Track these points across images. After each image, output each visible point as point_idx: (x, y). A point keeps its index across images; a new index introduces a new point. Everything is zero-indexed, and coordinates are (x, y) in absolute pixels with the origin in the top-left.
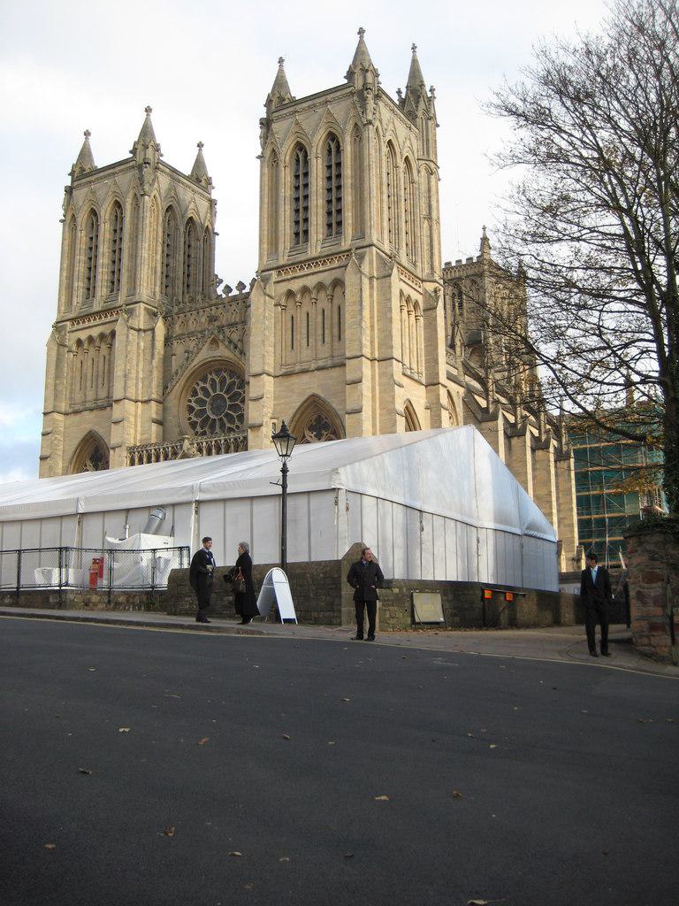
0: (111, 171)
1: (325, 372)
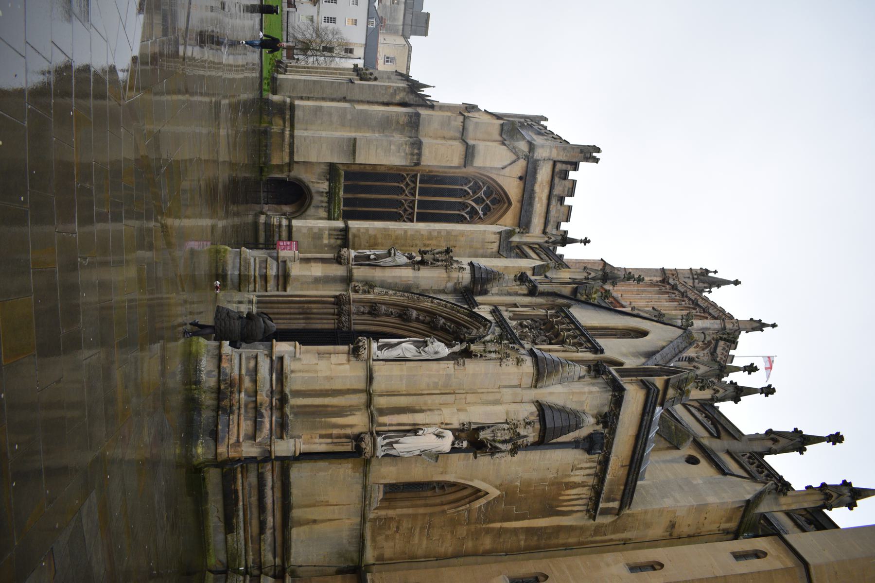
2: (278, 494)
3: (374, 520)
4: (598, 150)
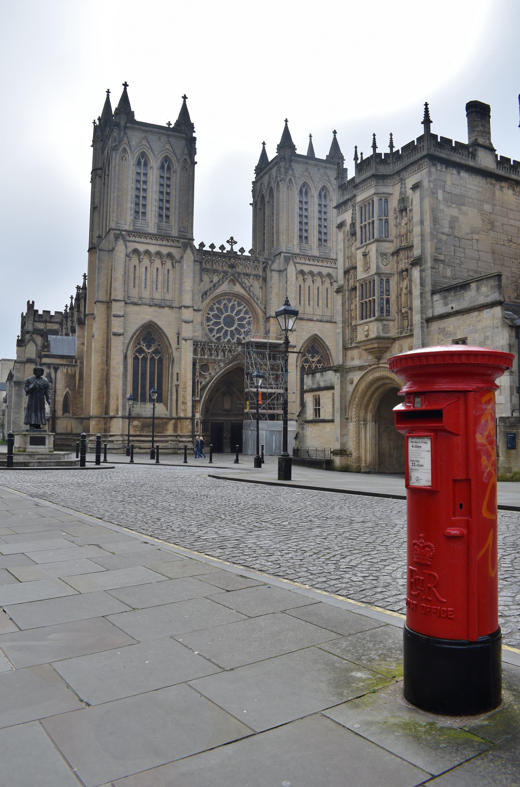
0: (164, 131)
1: (322, 323)
4: (28, 302)
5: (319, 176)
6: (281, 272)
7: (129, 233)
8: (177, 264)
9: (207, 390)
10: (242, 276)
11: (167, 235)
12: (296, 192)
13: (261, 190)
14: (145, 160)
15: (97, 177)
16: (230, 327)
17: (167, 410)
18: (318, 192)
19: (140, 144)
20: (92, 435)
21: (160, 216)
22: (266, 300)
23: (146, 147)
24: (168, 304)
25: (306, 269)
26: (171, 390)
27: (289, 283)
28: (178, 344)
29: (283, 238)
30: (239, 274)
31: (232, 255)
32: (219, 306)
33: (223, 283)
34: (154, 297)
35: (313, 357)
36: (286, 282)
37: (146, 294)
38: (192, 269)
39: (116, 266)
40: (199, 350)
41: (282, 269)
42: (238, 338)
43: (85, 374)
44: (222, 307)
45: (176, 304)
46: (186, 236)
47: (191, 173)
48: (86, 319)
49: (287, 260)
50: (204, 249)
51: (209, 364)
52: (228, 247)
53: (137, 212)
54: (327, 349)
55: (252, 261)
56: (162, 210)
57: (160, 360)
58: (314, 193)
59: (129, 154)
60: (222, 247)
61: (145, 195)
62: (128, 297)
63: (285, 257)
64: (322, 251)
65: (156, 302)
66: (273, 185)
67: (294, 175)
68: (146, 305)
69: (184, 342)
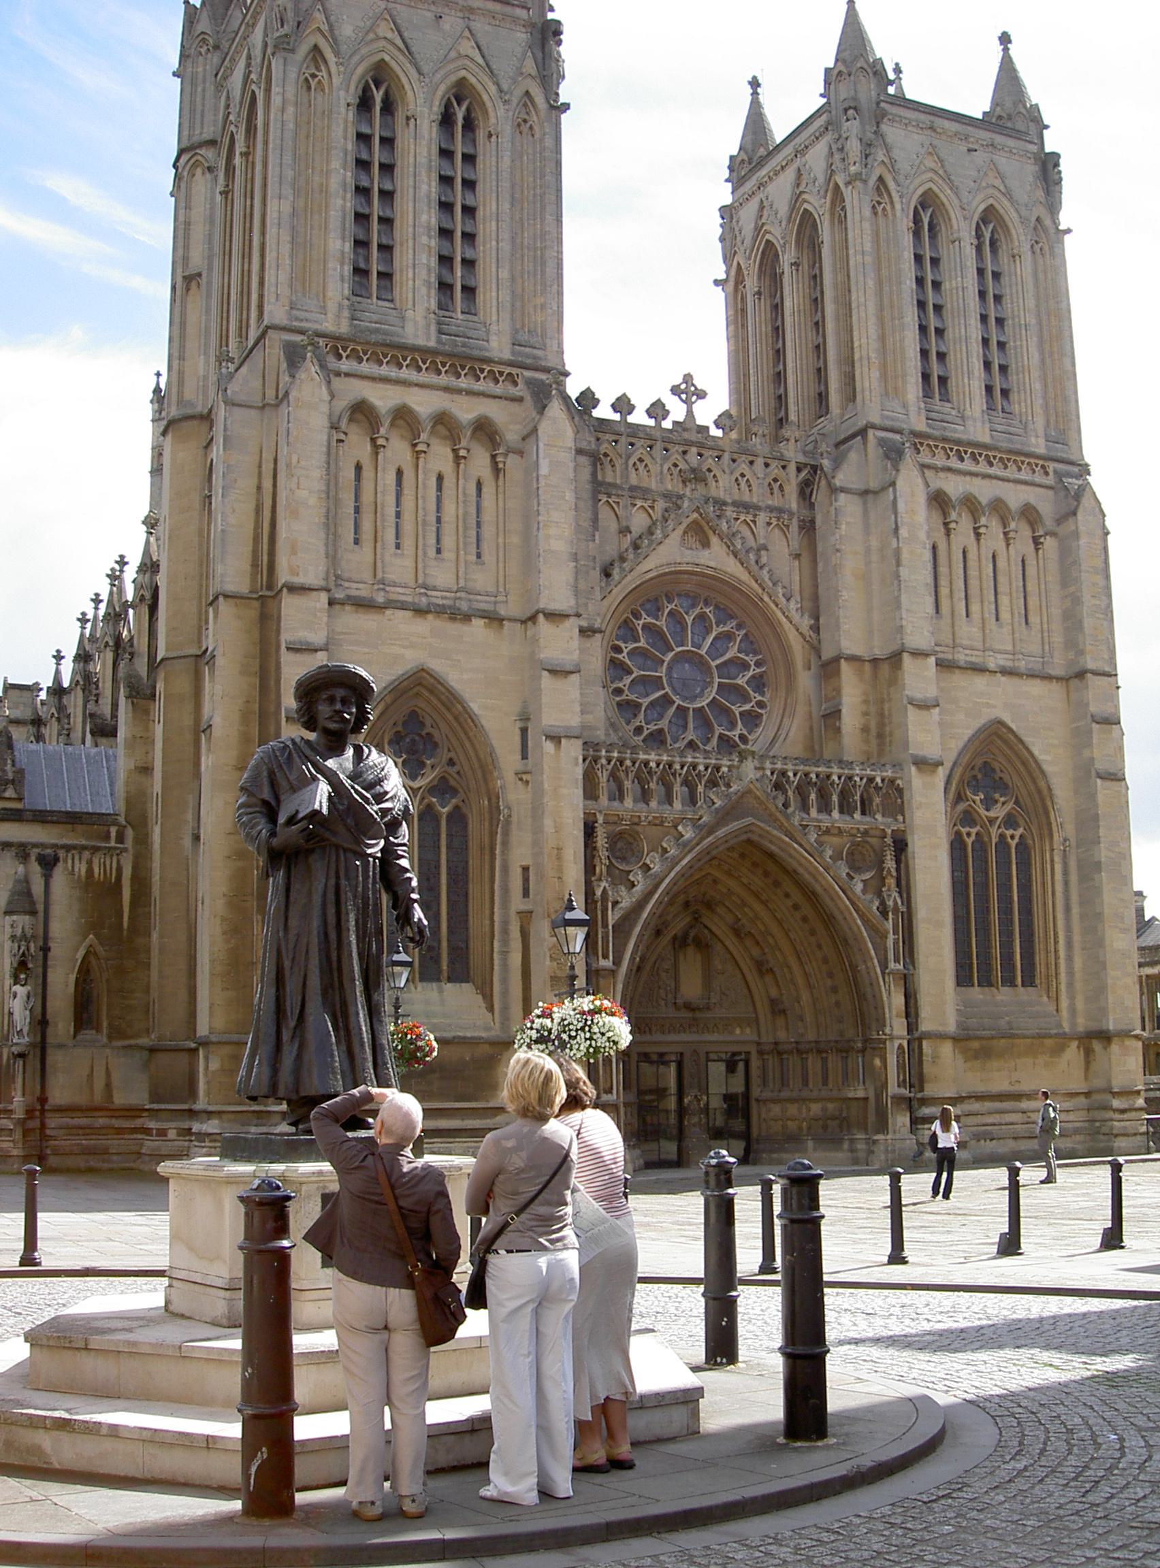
1: (1015, 681)
2: (79, 1114)
3: (110, 1038)
5: (974, 174)
6: (870, 497)
7: (338, 345)
8: (512, 461)
9: (637, 929)
10: (730, 512)
11: (476, 353)
12: (905, 223)
13: (758, 229)
14: (387, 94)
15: (199, 171)
16: (693, 699)
17: (491, 1009)
18: (974, 227)
19: (371, 36)
20: (210, 1114)
21: (445, 287)
22: (815, 598)
23: (390, 47)
24: (483, 606)
25: (954, 487)
26: (505, 932)
27: (903, 532)
28: (524, 757)
29: (868, 379)
30: (720, 504)
31: (694, 437)
32: (649, 620)
33: (666, 536)
34: (431, 581)
35: (989, 803)
36: (896, 530)
37: (399, 568)
38: (571, 475)
39: (294, 460)
40: (603, 777)
41: (874, 485)
42: (721, 736)
43: (156, 879)
44: (662, 623)
45: (512, 607)
46: (535, 357)
47: (549, 142)
48: (161, 676)
49: (893, 454)
50: (597, 413)
51: (639, 828)
52: (677, 411)
53: (360, 272)
54: (1037, 773)
55: (760, 462)
56: (452, 269)
57: (458, 818)
58: (961, 228)
59: (333, 69)
60: (657, 410)
61: (388, 214)
62: (337, 577)
63: (882, 442)
64: (1000, 428)
65: (437, 598)
66: (818, 204)
67: (892, 165)
68: (403, 606)
69: (549, 746)
